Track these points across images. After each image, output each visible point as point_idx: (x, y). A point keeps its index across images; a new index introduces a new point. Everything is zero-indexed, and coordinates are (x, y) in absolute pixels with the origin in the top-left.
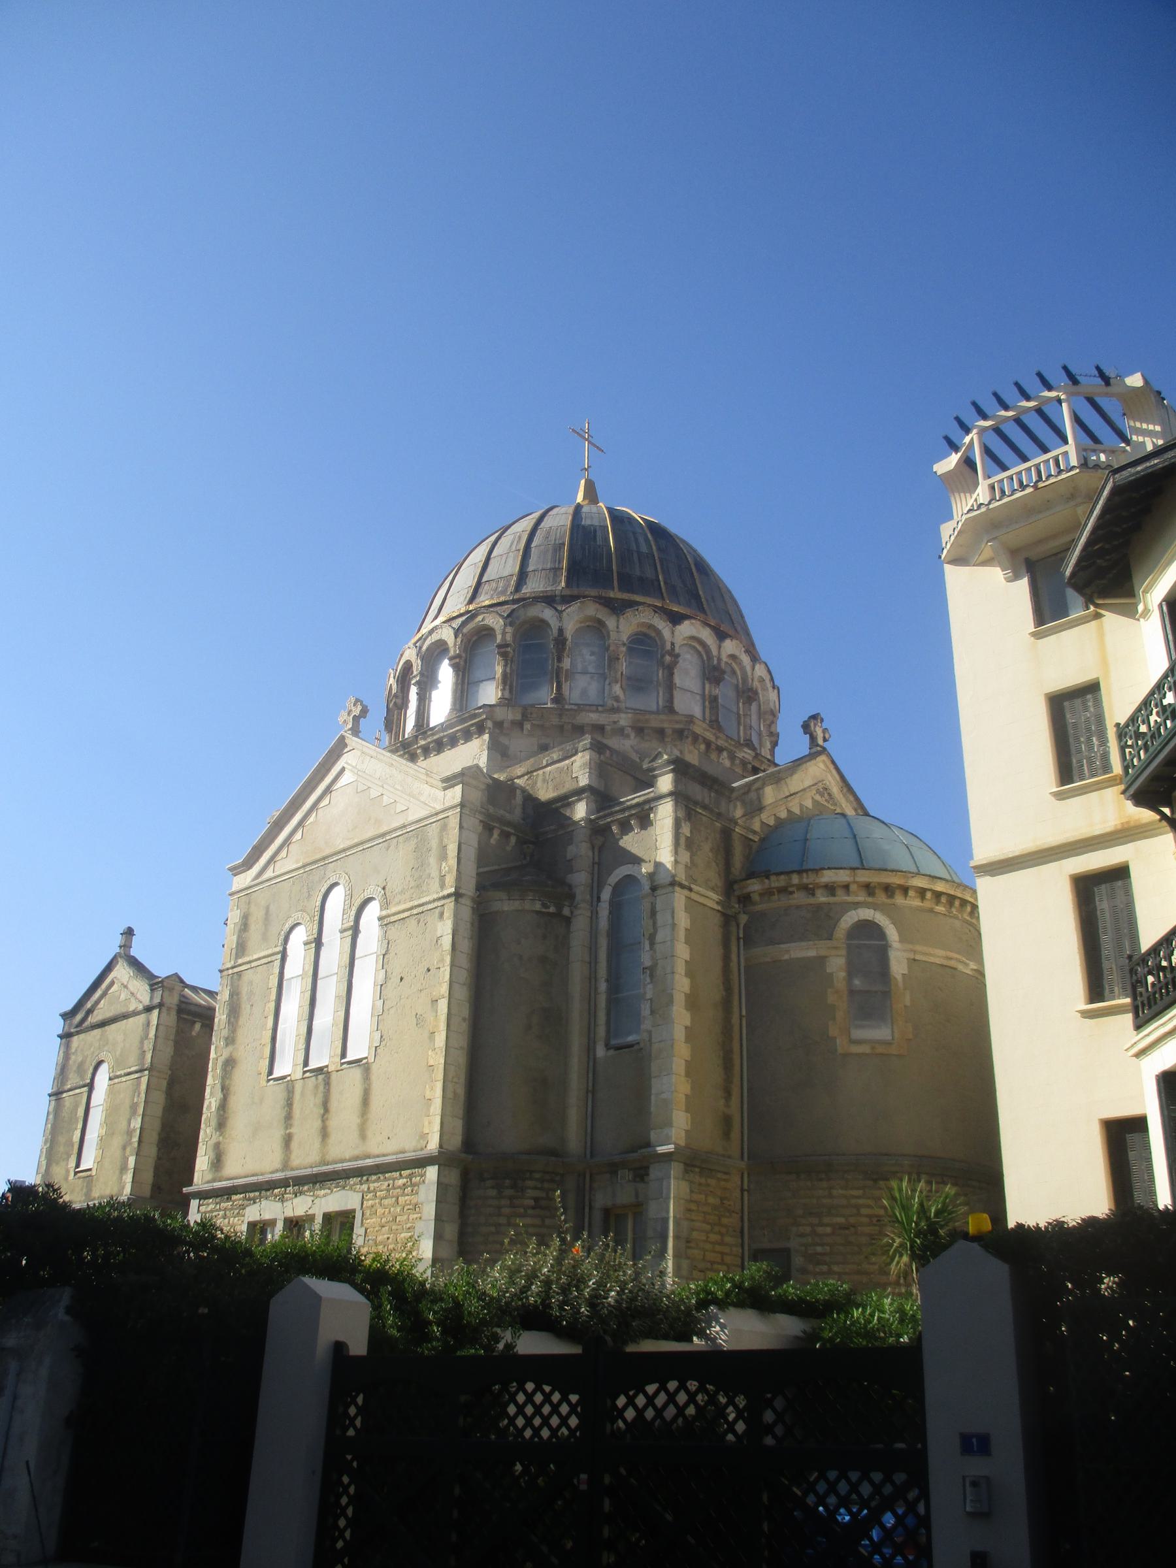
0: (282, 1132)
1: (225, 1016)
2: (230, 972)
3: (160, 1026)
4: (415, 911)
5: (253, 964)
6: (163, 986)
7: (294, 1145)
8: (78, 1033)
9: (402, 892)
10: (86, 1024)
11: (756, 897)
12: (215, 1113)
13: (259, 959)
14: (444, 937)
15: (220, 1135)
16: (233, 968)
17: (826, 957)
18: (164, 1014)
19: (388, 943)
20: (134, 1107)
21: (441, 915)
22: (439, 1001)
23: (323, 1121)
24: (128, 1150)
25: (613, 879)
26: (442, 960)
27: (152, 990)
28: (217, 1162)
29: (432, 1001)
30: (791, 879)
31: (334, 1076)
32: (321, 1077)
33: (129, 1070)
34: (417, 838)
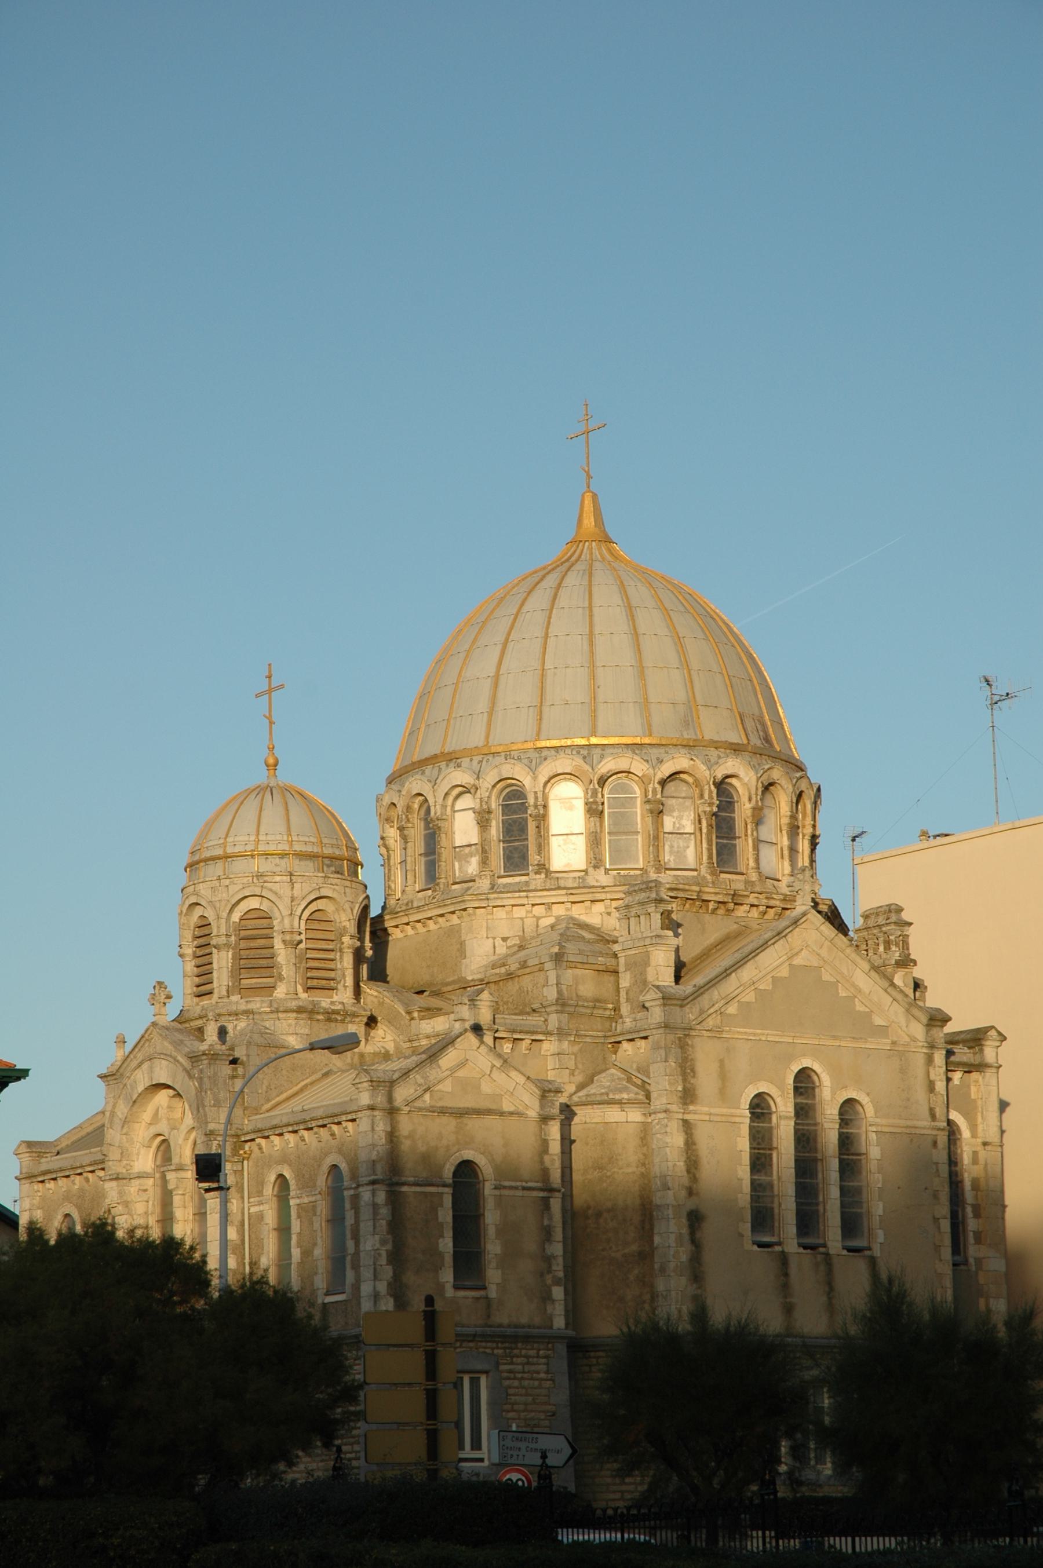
15: (699, 1288)
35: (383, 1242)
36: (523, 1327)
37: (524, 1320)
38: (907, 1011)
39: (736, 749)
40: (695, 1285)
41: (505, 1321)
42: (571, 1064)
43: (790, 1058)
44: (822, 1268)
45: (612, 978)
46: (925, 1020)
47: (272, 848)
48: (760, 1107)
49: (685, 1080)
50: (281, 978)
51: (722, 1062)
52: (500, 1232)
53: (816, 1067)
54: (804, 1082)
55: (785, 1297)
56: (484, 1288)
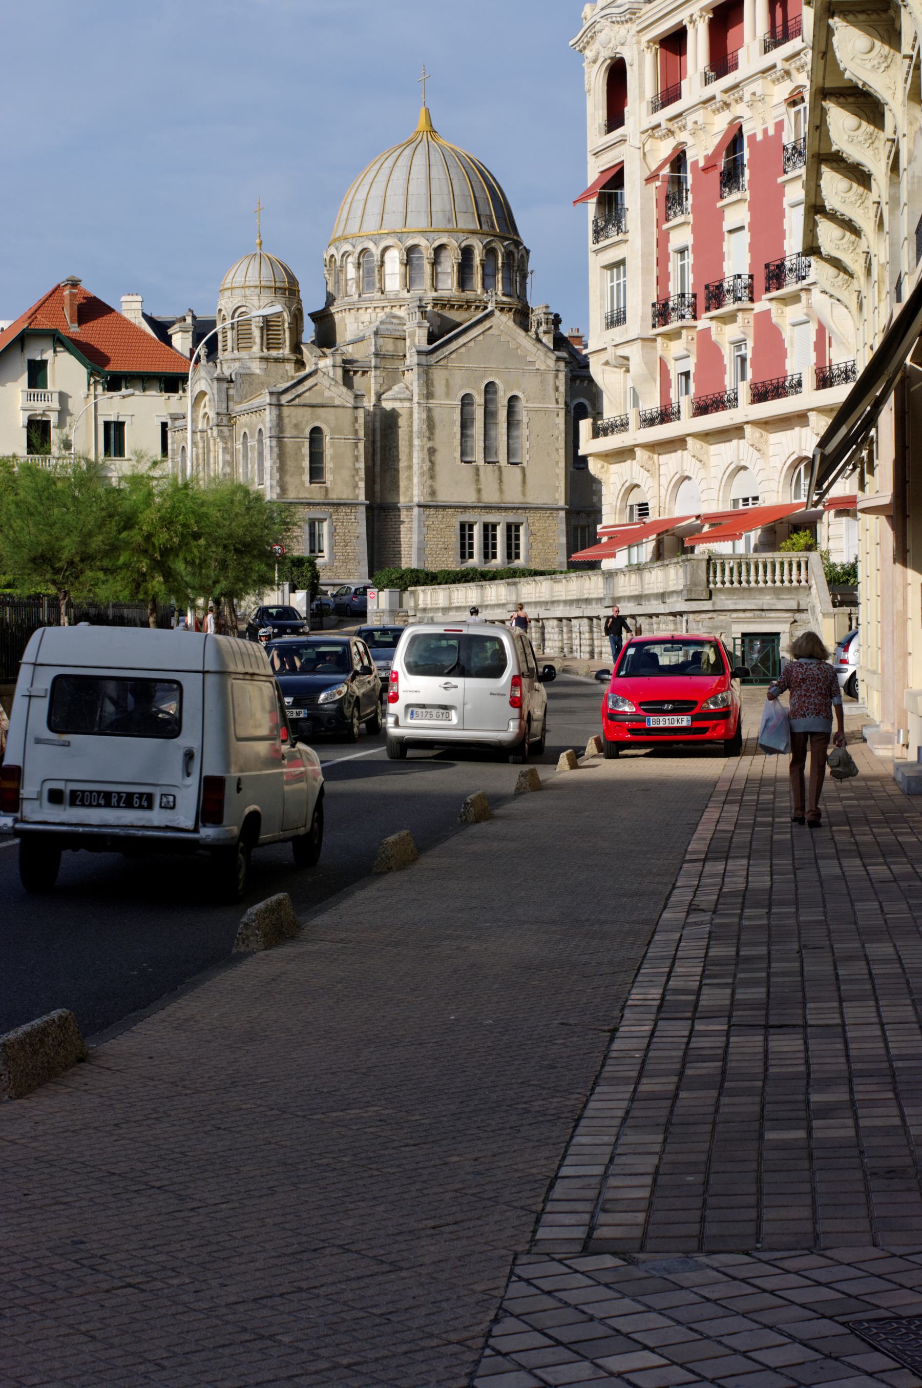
1: (425, 426)
7: (483, 493)
10: (294, 403)
21: (558, 415)
24: (357, 479)
31: (503, 469)
35: (275, 463)
37: (344, 496)
39: (473, 232)
41: (335, 497)
42: (381, 381)
43: (483, 377)
44: (497, 472)
45: (403, 342)
47: (251, 284)
48: (466, 401)
49: (428, 389)
50: (255, 343)
51: (447, 380)
52: (333, 458)
53: (497, 381)
54: (490, 388)
56: (324, 483)
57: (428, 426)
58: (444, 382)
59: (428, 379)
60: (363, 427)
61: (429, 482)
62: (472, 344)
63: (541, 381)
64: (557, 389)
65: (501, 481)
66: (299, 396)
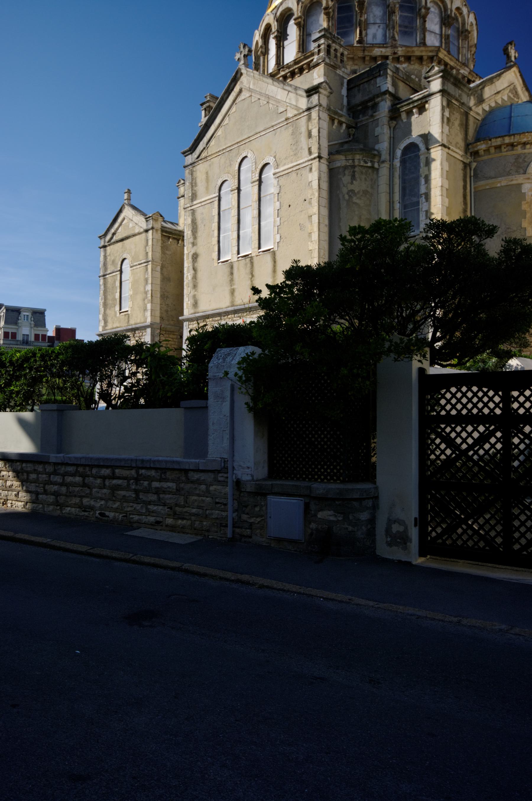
0: (229, 288)
1: (190, 232)
2: (190, 208)
3: (154, 240)
4: (294, 169)
5: (203, 204)
6: (152, 219)
7: (236, 294)
8: (109, 245)
9: (286, 158)
10: (113, 241)
11: (482, 152)
12: (191, 281)
13: (206, 201)
14: (312, 182)
15: (195, 291)
16: (191, 206)
17: (522, 184)
18: (154, 233)
19: (280, 187)
20: (146, 280)
21: (311, 169)
22: (313, 216)
23: (252, 281)
24: (146, 301)
25: (403, 145)
26: (313, 194)
27: (147, 221)
28: (195, 304)
29: (309, 217)
30: (504, 140)
31: (255, 259)
32: (248, 260)
33: (140, 262)
34: (293, 127)
36: (138, 324)
37: (138, 321)
38: (297, 94)
40: (194, 290)
43: (238, 154)
44: (249, 265)
46: (304, 94)
49: (192, 190)
51: (207, 173)
55: (231, 286)
57: (192, 231)
58: (204, 176)
59: (192, 179)
60: (151, 249)
61: (193, 293)
62: (226, 121)
63: (293, 134)
64: (310, 135)
65: (253, 276)
66: (114, 234)
